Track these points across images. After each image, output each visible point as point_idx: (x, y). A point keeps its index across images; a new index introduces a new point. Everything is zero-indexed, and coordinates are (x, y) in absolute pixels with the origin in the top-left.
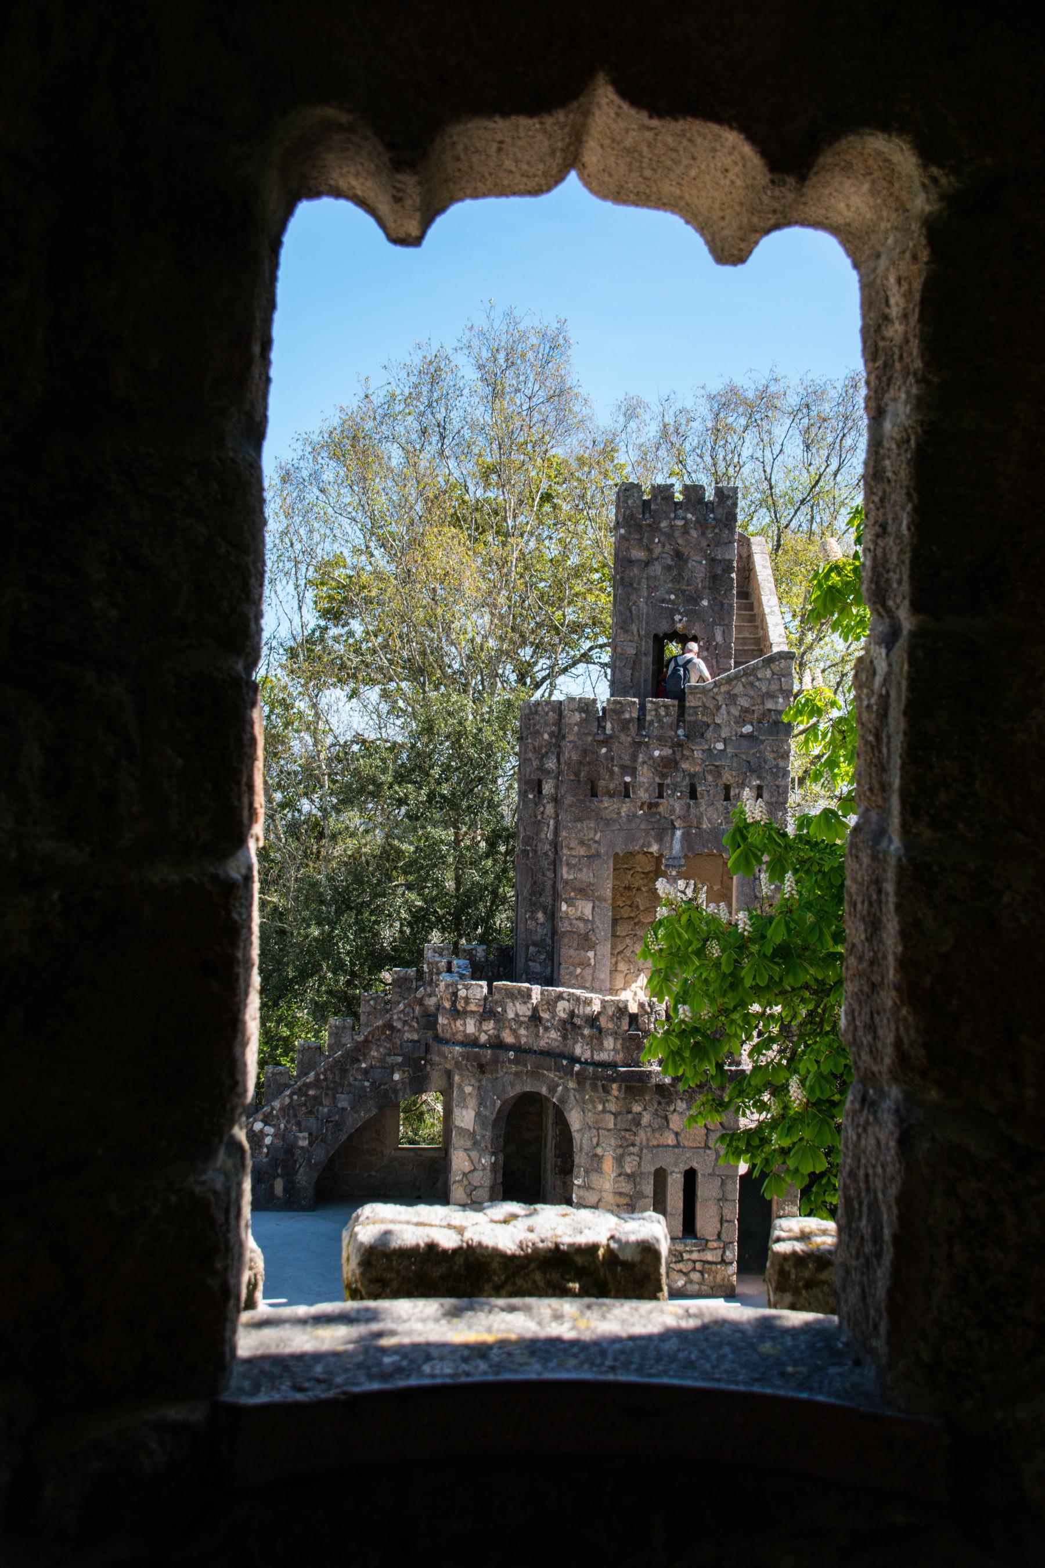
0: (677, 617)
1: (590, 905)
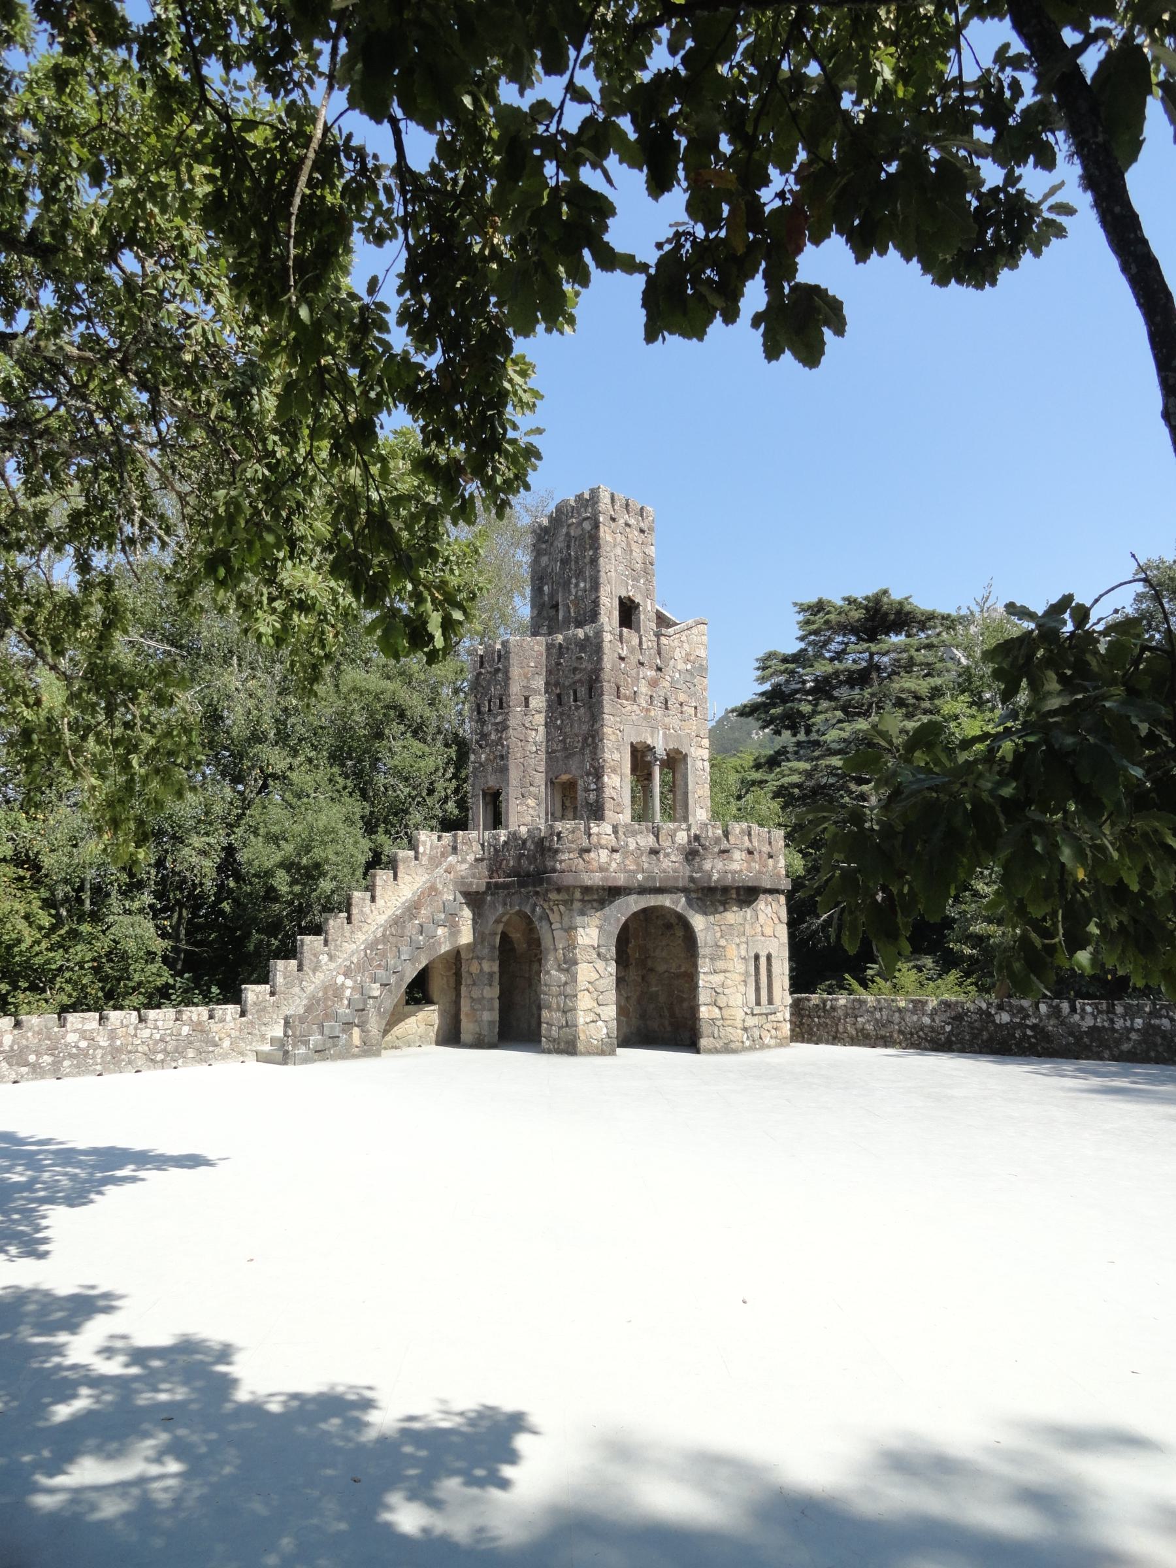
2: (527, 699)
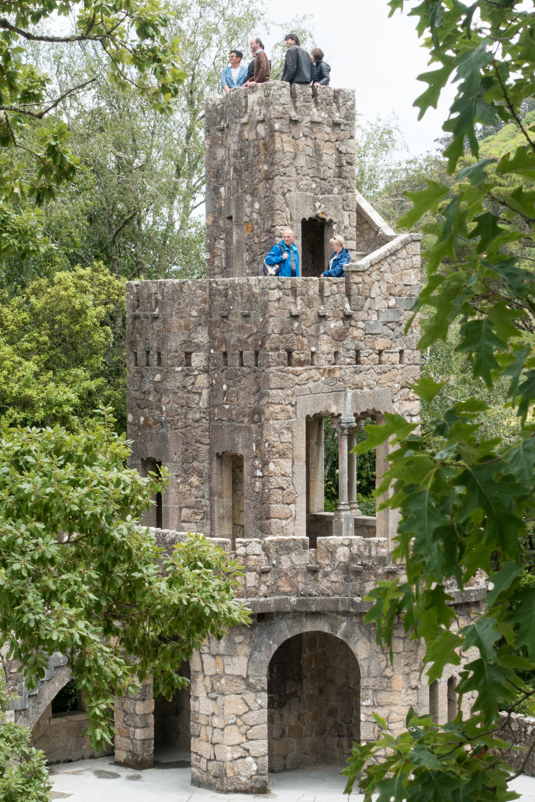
1: (290, 464)
2: (188, 355)
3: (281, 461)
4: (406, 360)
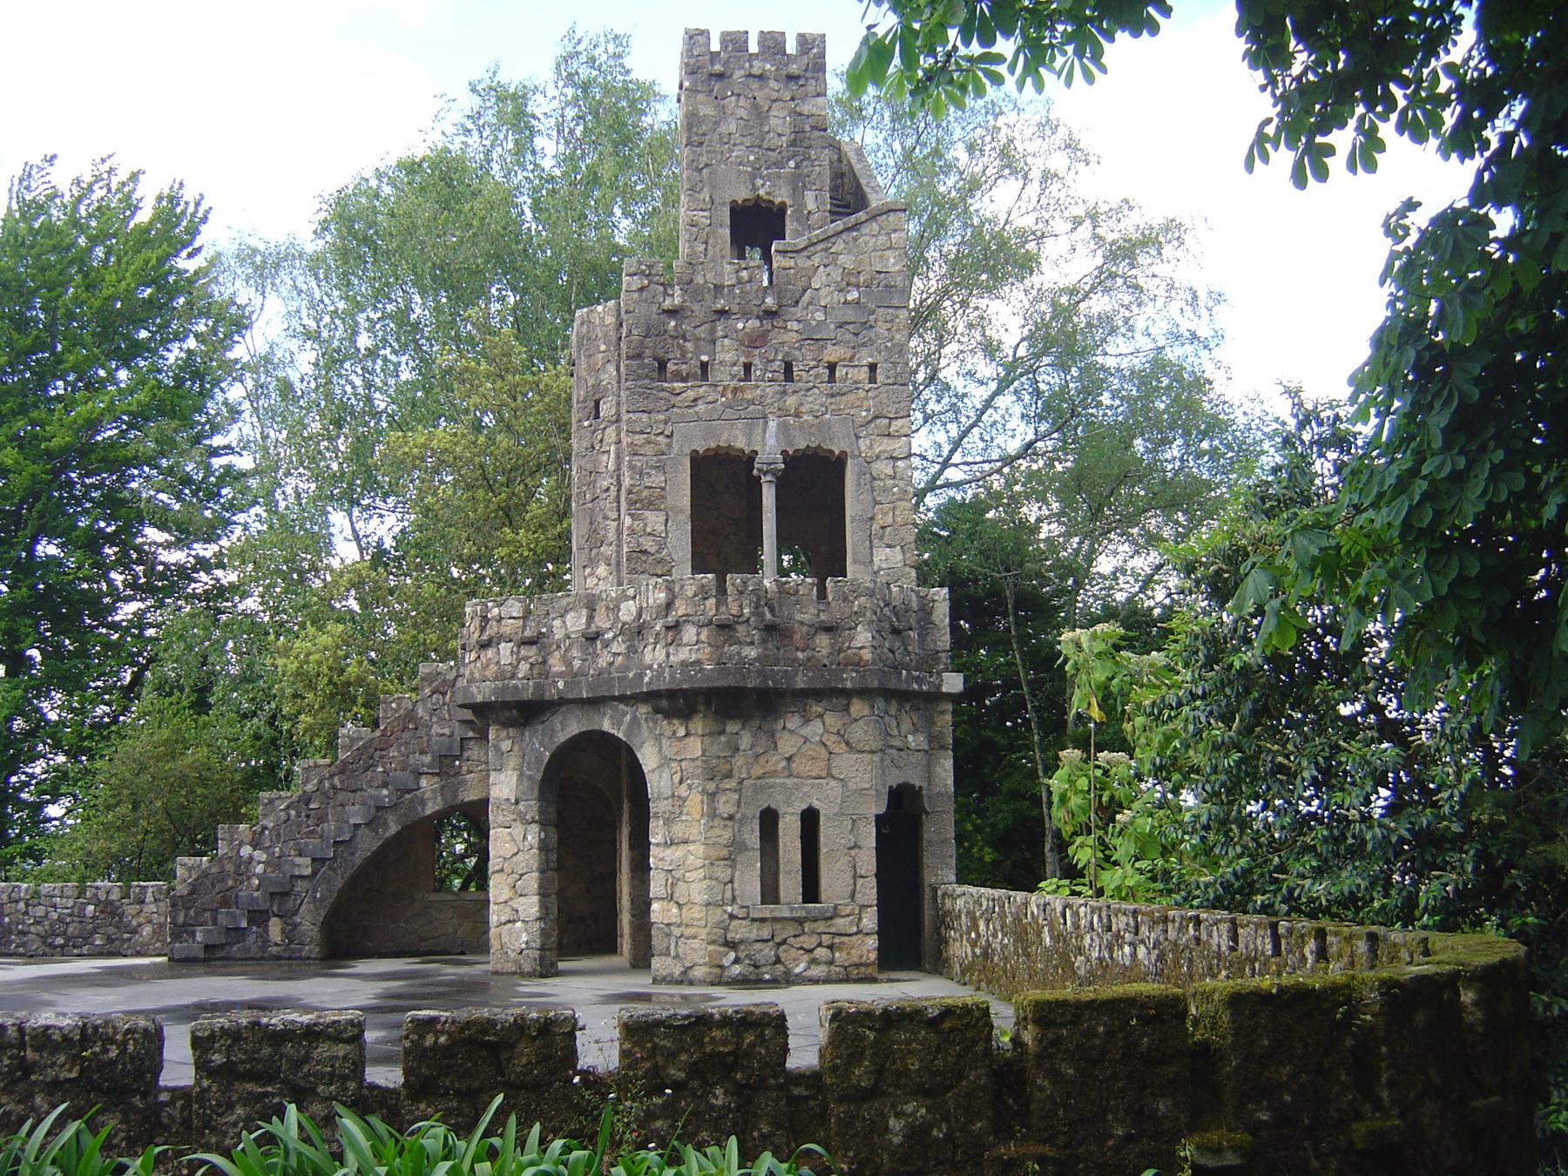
0: (759, 182)
3: (647, 513)
4: (880, 378)
